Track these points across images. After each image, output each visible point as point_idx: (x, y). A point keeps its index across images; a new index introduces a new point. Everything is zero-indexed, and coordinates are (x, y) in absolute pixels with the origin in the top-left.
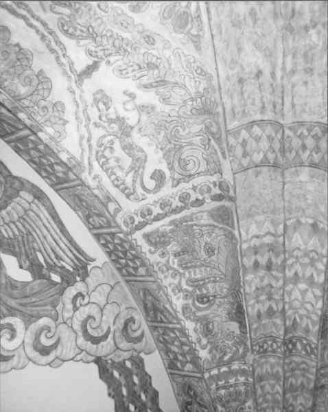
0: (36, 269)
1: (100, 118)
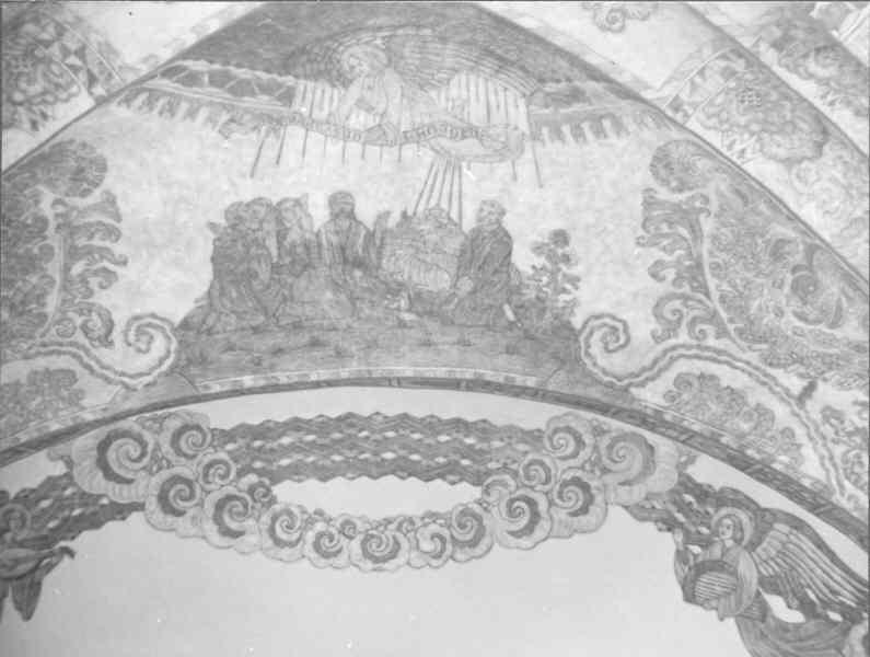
0: (806, 606)
1: (837, 433)
